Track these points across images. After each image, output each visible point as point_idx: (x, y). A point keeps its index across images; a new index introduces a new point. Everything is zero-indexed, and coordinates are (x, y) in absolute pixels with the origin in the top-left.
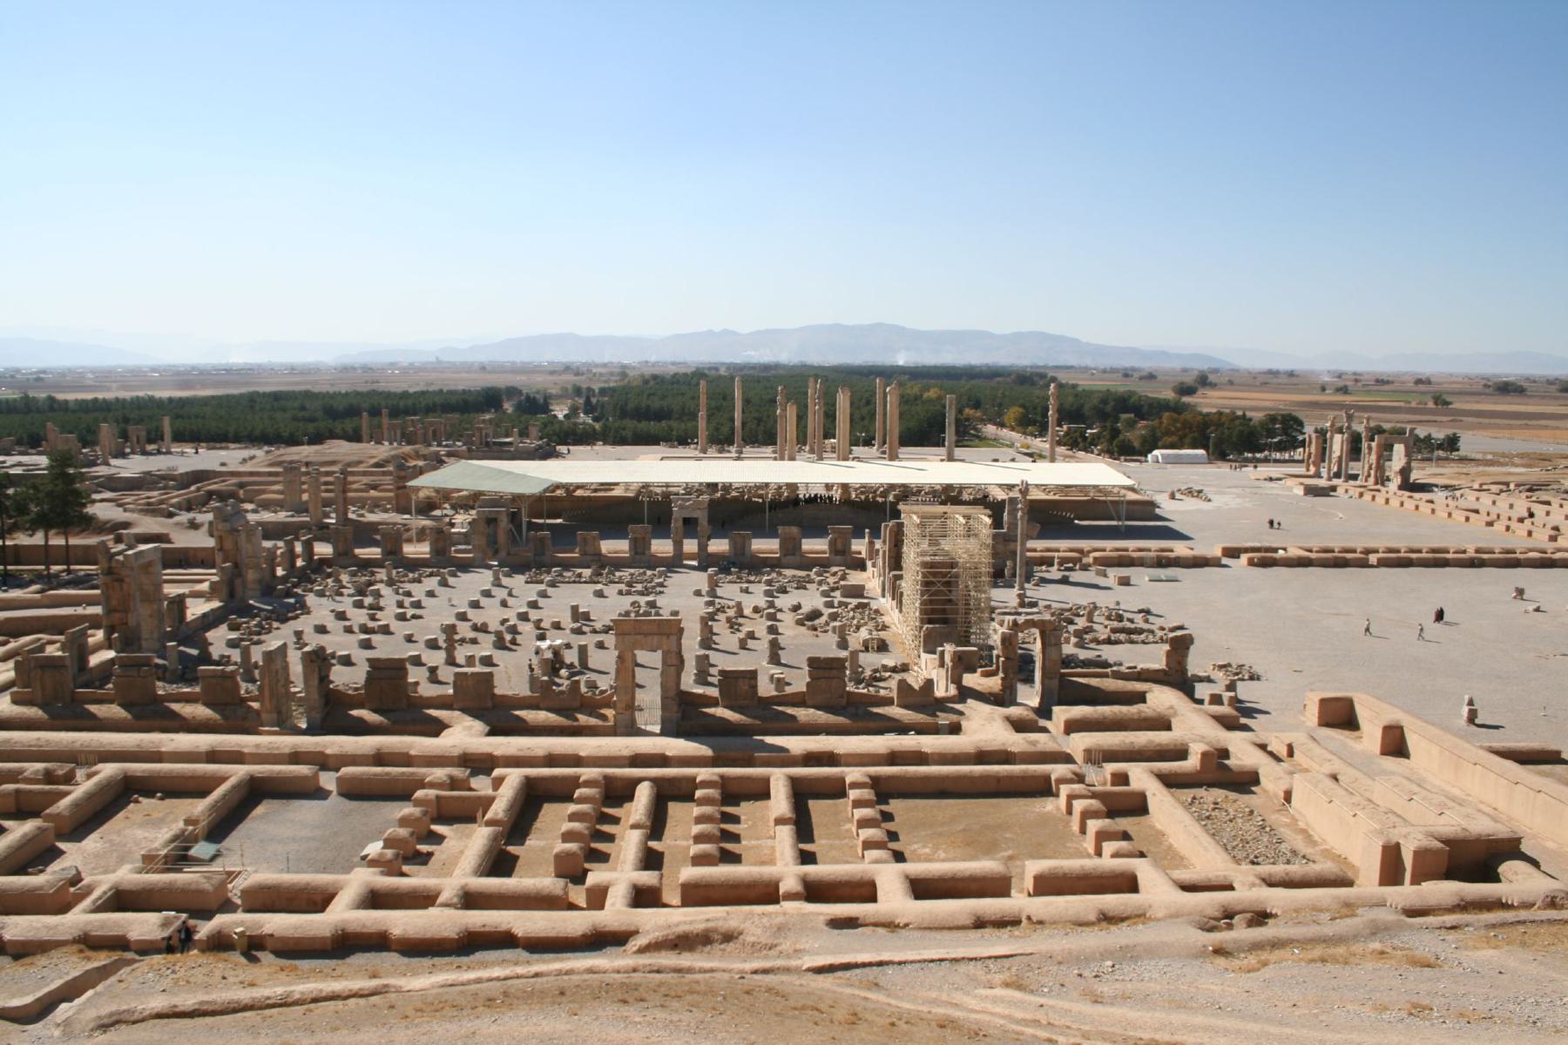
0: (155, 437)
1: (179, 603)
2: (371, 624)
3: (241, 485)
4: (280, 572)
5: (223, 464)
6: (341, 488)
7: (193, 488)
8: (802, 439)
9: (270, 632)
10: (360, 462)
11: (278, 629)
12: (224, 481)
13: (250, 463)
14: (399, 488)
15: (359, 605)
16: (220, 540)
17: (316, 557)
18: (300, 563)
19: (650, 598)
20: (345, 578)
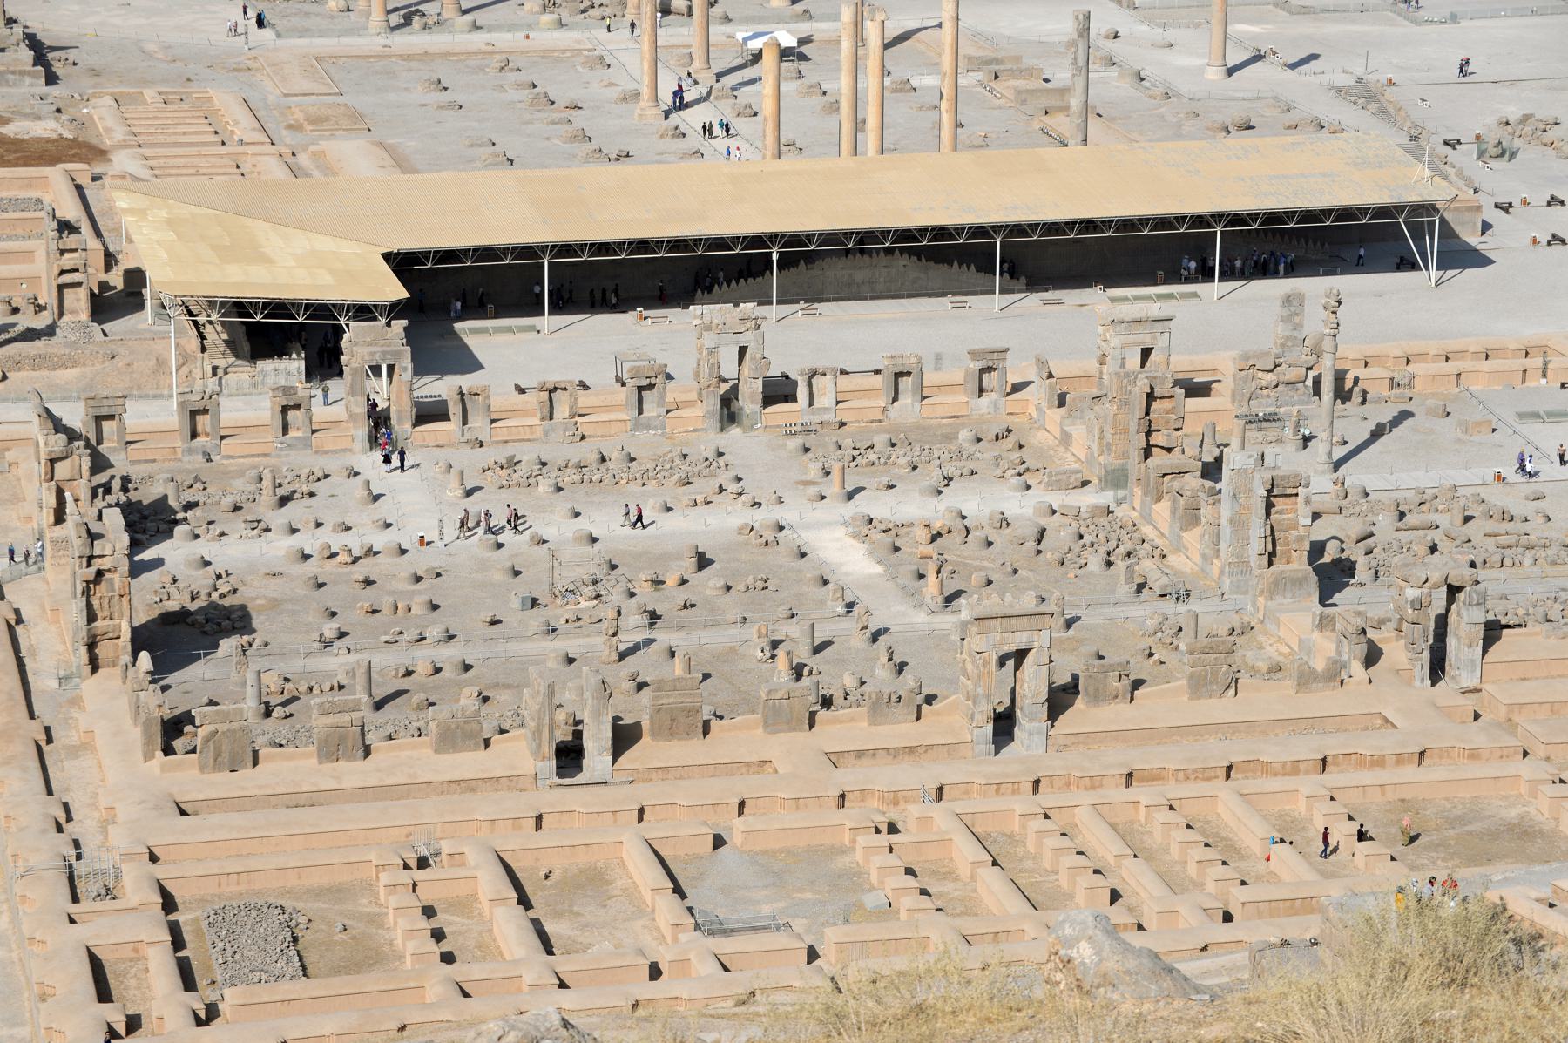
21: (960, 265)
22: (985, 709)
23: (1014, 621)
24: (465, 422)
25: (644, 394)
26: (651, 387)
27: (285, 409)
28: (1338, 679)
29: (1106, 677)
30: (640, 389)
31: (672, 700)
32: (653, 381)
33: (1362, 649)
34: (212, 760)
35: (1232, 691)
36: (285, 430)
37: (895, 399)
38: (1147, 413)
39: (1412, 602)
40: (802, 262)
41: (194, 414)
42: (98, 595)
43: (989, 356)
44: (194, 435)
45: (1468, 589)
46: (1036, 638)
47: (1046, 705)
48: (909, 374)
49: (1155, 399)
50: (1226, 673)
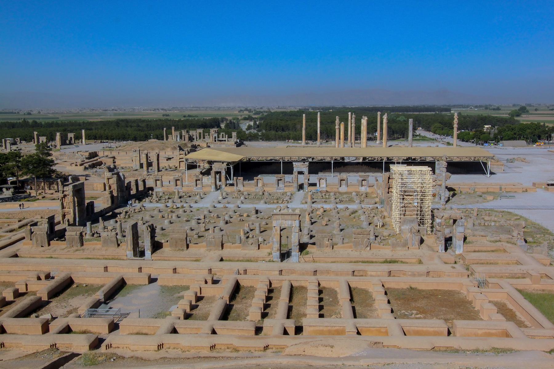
0: (78, 137)
1: (91, 205)
7: (95, 158)
8: (346, 138)
14: (180, 159)
19: (286, 204)
21: (378, 169)
22: (276, 246)
23: (286, 216)
24: (237, 186)
25: (279, 181)
26: (281, 180)
27: (196, 180)
28: (407, 247)
29: (323, 240)
30: (278, 180)
31: (176, 236)
32: (281, 179)
33: (418, 238)
34: (35, 243)
35: (369, 248)
36: (196, 186)
37: (340, 186)
38: (388, 183)
39: (438, 224)
40: (342, 166)
41: (176, 180)
42: (66, 202)
43: (364, 177)
44: (176, 186)
45: (458, 220)
46: (294, 223)
47: (298, 247)
48: (344, 180)
49: (390, 179)
50: (366, 241)
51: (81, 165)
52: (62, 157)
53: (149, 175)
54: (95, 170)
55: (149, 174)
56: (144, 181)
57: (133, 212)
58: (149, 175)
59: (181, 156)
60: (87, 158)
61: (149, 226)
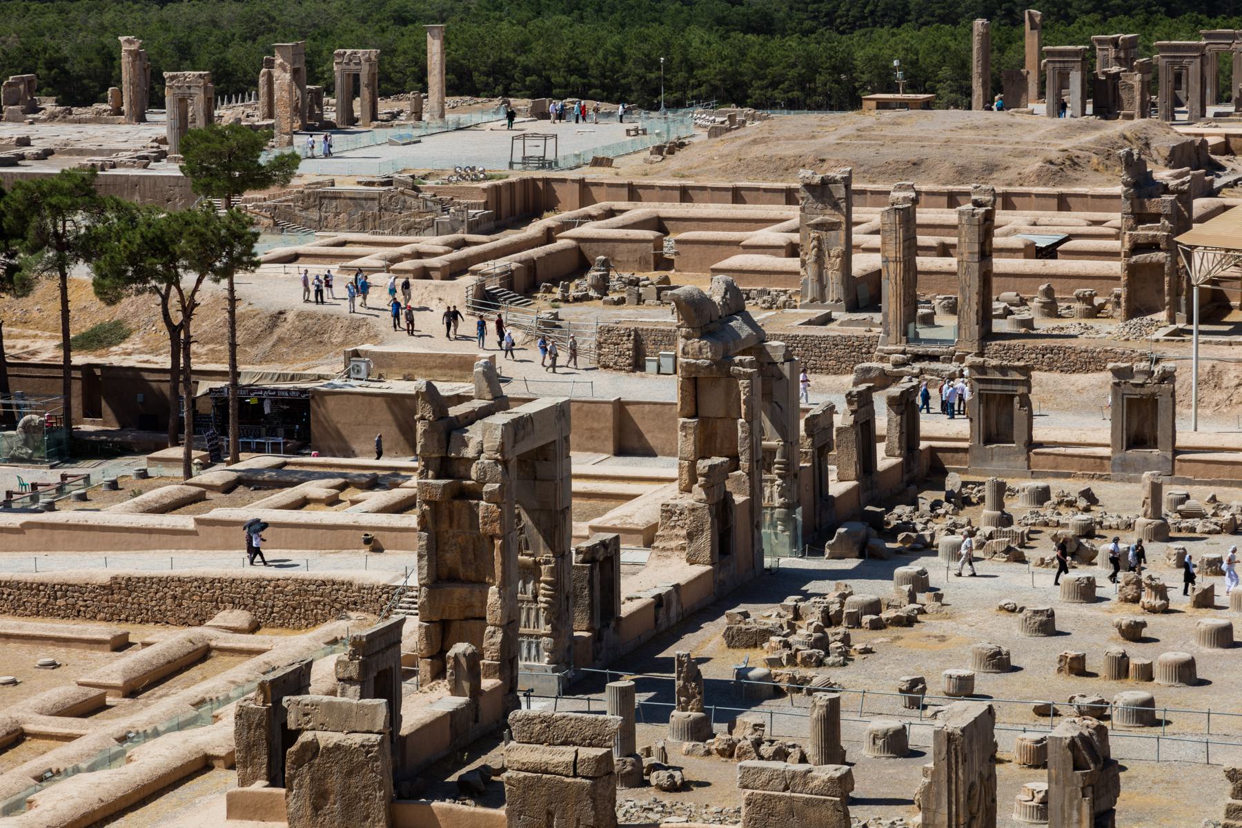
2: (1138, 655)
3: (659, 224)
4: (836, 488)
5: (598, 162)
6: (976, 248)
7: (535, 229)
9: (846, 658)
10: (990, 168)
11: (867, 651)
12: (611, 213)
13: (675, 162)
14: (1137, 248)
15: (1087, 592)
16: (694, 384)
17: (923, 445)
18: (884, 460)
20: (1017, 506)
51: (454, 271)
52: (314, 214)
53: (918, 358)
54: (541, 307)
55: (920, 349)
56: (907, 408)
57: (866, 619)
58: (918, 358)
59: (1146, 232)
60: (474, 227)
61: (1081, 736)
